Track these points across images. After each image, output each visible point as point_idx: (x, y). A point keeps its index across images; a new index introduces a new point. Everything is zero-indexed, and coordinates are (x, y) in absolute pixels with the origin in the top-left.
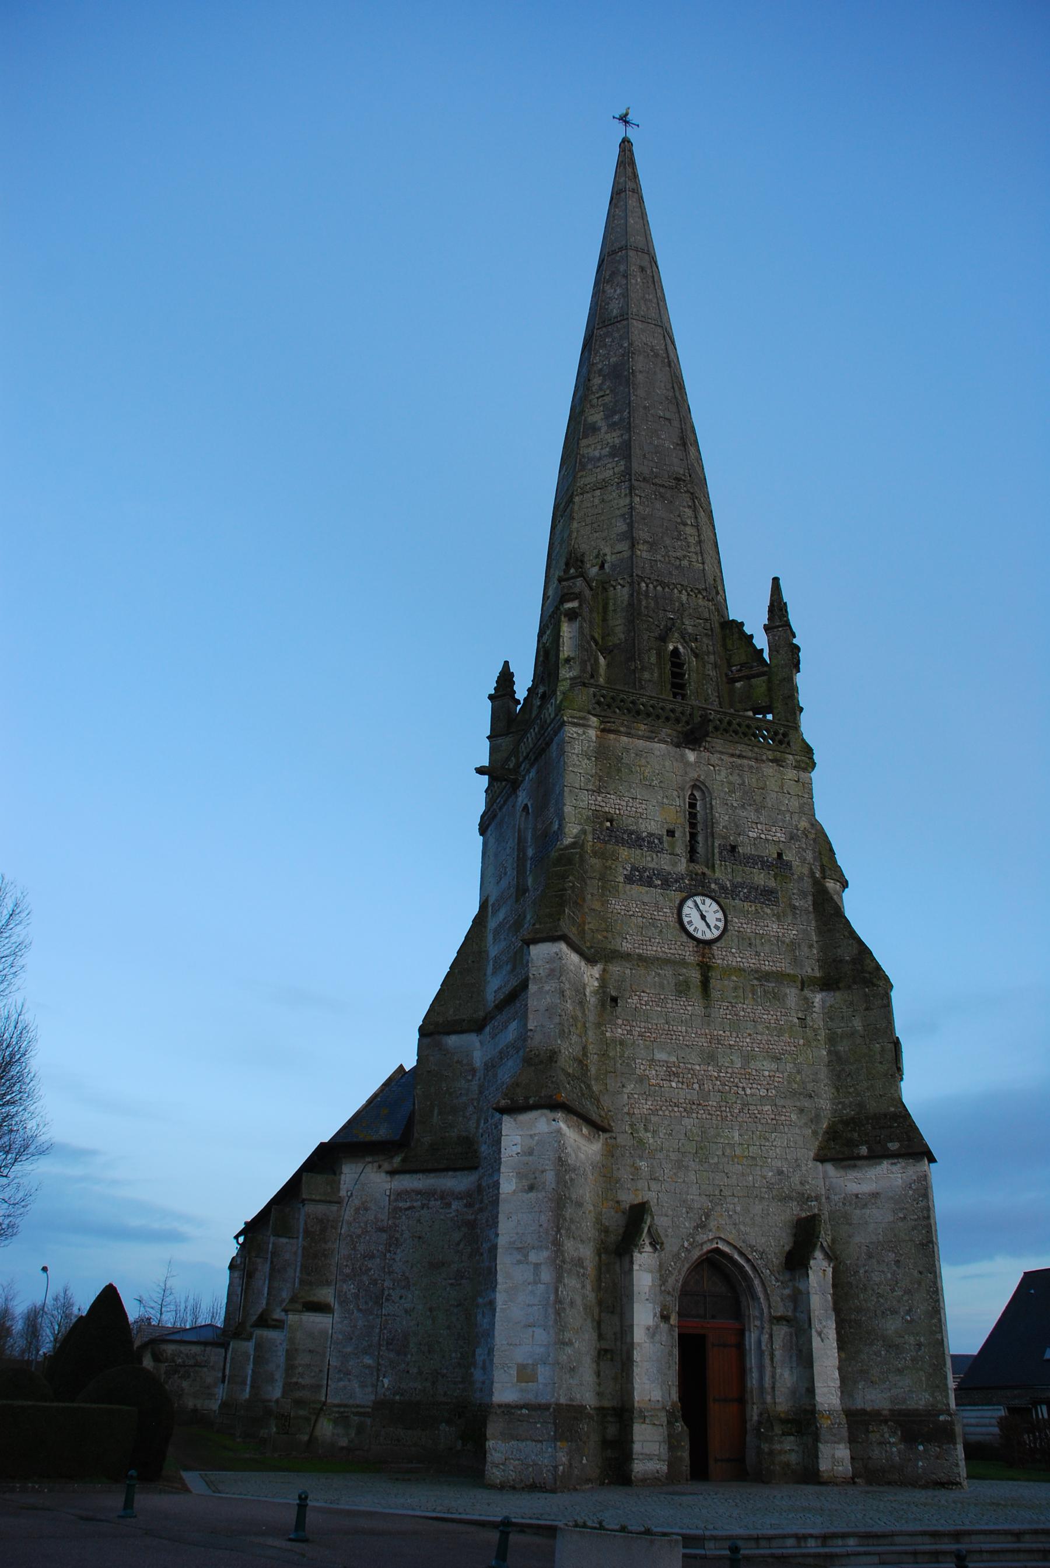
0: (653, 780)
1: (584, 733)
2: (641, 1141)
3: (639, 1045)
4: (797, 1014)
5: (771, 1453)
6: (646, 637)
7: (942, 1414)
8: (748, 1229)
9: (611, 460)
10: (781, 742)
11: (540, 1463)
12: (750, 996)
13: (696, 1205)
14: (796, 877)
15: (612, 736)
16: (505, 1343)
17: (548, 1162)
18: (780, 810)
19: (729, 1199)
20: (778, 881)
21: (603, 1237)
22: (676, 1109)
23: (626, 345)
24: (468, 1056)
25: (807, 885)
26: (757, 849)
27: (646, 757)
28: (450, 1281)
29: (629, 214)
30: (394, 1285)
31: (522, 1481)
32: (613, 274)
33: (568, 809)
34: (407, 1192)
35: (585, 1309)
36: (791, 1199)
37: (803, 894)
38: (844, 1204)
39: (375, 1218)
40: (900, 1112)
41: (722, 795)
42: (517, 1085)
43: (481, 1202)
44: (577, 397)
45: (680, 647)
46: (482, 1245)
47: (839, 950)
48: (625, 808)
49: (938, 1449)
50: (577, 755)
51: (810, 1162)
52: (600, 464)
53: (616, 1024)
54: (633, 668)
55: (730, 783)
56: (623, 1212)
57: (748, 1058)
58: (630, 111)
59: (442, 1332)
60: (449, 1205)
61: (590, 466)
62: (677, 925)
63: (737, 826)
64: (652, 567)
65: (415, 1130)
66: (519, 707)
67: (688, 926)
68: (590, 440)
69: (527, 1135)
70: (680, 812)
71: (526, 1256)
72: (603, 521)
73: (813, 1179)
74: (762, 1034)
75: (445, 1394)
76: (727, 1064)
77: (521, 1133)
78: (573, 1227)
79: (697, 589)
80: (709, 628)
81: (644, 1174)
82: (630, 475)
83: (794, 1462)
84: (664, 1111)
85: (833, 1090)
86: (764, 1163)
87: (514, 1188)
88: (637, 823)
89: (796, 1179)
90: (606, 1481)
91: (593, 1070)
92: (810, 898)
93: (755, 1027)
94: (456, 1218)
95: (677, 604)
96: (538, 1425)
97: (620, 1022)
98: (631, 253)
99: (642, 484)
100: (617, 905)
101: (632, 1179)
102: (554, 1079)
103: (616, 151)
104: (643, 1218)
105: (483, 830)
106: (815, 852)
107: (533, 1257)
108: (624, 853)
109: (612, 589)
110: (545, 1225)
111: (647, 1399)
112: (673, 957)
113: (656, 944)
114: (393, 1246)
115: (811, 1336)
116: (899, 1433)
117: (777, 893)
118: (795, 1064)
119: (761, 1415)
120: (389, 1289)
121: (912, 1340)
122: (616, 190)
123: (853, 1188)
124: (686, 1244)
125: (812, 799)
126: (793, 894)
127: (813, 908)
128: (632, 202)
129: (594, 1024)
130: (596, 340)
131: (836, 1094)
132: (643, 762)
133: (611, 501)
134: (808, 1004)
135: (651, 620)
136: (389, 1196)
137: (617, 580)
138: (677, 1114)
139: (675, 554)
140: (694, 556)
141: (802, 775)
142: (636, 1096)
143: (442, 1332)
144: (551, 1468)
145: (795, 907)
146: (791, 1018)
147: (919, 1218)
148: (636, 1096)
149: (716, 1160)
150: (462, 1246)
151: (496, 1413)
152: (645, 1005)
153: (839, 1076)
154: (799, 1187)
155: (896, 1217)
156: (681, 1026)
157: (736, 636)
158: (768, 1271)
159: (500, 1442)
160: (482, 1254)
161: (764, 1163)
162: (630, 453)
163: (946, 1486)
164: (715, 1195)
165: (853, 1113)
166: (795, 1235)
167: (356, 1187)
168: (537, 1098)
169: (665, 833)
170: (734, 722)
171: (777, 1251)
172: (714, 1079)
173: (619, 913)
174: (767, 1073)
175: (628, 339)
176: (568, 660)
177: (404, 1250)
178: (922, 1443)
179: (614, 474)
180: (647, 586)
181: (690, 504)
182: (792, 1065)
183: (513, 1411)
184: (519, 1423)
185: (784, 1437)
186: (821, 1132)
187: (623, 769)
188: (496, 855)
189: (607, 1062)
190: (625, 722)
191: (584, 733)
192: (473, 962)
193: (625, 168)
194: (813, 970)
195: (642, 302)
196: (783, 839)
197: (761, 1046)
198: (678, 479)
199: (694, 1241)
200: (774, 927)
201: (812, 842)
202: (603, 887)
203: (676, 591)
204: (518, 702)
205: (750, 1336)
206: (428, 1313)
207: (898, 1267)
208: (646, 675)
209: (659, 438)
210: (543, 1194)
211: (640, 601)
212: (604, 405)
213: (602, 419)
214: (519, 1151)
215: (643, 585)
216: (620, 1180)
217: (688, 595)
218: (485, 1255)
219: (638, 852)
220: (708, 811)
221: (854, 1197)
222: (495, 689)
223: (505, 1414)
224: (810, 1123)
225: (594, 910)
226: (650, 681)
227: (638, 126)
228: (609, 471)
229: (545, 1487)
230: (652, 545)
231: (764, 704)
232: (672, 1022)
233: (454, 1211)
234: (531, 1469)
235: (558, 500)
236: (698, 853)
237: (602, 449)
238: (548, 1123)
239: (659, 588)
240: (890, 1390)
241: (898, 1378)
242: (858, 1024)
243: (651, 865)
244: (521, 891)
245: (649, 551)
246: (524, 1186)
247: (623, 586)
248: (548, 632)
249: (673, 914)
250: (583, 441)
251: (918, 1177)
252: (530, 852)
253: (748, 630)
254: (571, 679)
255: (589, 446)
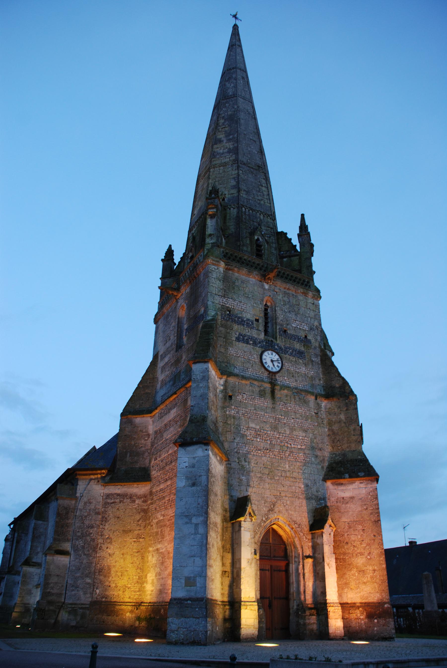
0: (249, 295)
1: (218, 269)
2: (243, 466)
3: (242, 419)
4: (314, 410)
5: (305, 624)
6: (245, 231)
7: (386, 604)
8: (293, 513)
9: (228, 154)
10: (306, 285)
11: (198, 629)
12: (293, 400)
13: (269, 500)
14: (313, 347)
15: (230, 272)
16: (178, 565)
17: (202, 471)
18: (306, 316)
19: (284, 498)
20: (305, 348)
21: (224, 513)
22: (259, 452)
23: (236, 107)
24: (146, 428)
25: (318, 351)
26: (295, 332)
27: (246, 284)
28: (134, 540)
29: (237, 55)
30: (103, 541)
31: (187, 639)
32: (230, 78)
33: (209, 303)
34: (112, 494)
35: (218, 549)
36: (312, 499)
37: (316, 355)
38: (337, 502)
39: (95, 507)
40: (363, 459)
41: (280, 305)
42: (186, 432)
43: (152, 499)
44: (211, 129)
45: (260, 238)
46: (152, 521)
47: (333, 382)
48: (236, 306)
49: (384, 621)
50: (215, 278)
51: (320, 482)
52: (223, 156)
53: (231, 408)
54: (239, 244)
55: (284, 301)
56: (234, 502)
57: (292, 429)
58: (238, 13)
59: (129, 565)
60: (134, 501)
61: (218, 157)
62: (260, 363)
63: (287, 321)
64: (247, 201)
65: (117, 464)
66: (175, 267)
67: (265, 364)
68: (218, 145)
69: (192, 457)
70: (261, 311)
71: (191, 520)
72: (224, 180)
73: (322, 490)
74: (299, 419)
75: (129, 598)
76: (283, 432)
77: (188, 456)
78: (214, 506)
79: (268, 214)
80: (273, 232)
81: (244, 483)
82: (238, 161)
83: (315, 629)
84: (254, 453)
85: (331, 448)
86: (300, 481)
87: (184, 484)
88: (241, 314)
89: (314, 489)
90: (226, 640)
91: (220, 429)
92: (319, 357)
93: (295, 415)
94: (138, 508)
95: (259, 219)
96: (197, 609)
97: (233, 407)
98: (238, 71)
99: (243, 166)
100: (232, 351)
101: (239, 485)
102: (206, 430)
103: (231, 30)
104: (246, 504)
105: (156, 321)
106: (321, 337)
107: (194, 520)
108: (236, 327)
109: (228, 209)
110: (201, 504)
111: (248, 596)
112: (258, 378)
113: (250, 372)
114: (104, 522)
115: (324, 566)
116: (365, 613)
117: (305, 353)
118: (313, 434)
119: (298, 605)
120: (101, 543)
121: (371, 568)
122: (231, 45)
123: (342, 494)
124: (264, 519)
125: (320, 312)
126: (312, 355)
127: (321, 362)
128: (238, 50)
129: (221, 407)
130: (221, 104)
131: (332, 450)
132: (245, 286)
133: (228, 172)
134: (319, 406)
135: (247, 224)
136: (103, 496)
137: (231, 205)
138: (260, 455)
139: (257, 198)
140: (266, 200)
141: (315, 301)
142: (241, 444)
143: (129, 565)
144: (204, 632)
145: (312, 361)
146: (311, 412)
147: (373, 509)
148: (241, 444)
149: (278, 478)
150: (140, 522)
151: (173, 603)
152: (245, 400)
153: (333, 442)
154: (315, 493)
155: (362, 509)
156: (262, 412)
157: (283, 238)
158: (302, 534)
159: (175, 619)
160: (152, 526)
161: (300, 481)
162: (238, 152)
163: (388, 639)
164: (277, 495)
165: (340, 459)
166: (314, 516)
167: (85, 491)
168: (198, 438)
169: (254, 320)
170: (286, 273)
171: (306, 524)
172: (277, 439)
173: (233, 355)
174: (301, 438)
175: (237, 105)
176: (210, 235)
177: (109, 524)
178: (376, 618)
179: (230, 160)
180: (245, 209)
181: (264, 178)
182: (312, 435)
183: (183, 602)
184: (186, 608)
185: (310, 617)
186: (325, 468)
187: (235, 288)
188: (164, 332)
189: (227, 426)
190: (237, 266)
191: (218, 269)
192: (150, 383)
193: (235, 36)
194: (321, 390)
195: (243, 91)
196: (307, 329)
197: (298, 424)
198: (259, 166)
199: (268, 518)
200: (303, 370)
201: (320, 332)
202: (226, 342)
203: (258, 214)
204: (175, 264)
205: (293, 566)
206: (122, 556)
207: (364, 532)
208: (245, 248)
209: (250, 148)
210: (200, 487)
211: (242, 215)
212: (225, 131)
213: (224, 137)
214: (187, 465)
215: (244, 209)
216: (233, 485)
217: (264, 216)
218: (154, 526)
219: (242, 327)
220: (274, 312)
221: (342, 499)
222: (165, 257)
223: (178, 604)
224: (320, 463)
225: (221, 352)
226: (246, 251)
227: (241, 21)
228: (228, 158)
229: (200, 643)
230: (248, 192)
231: (297, 269)
232: (258, 410)
233: (137, 504)
234: (192, 633)
235: (200, 173)
236: (269, 332)
237: (224, 149)
238: (203, 451)
239: (251, 211)
240: (360, 592)
241: (364, 587)
242: (342, 417)
243: (248, 334)
244: (179, 346)
245: (246, 195)
246: (190, 483)
247: (234, 208)
248: (194, 229)
249: (258, 358)
250: (215, 146)
251: (373, 489)
252: (185, 327)
253: (289, 236)
254: (212, 243)
255: (217, 148)
